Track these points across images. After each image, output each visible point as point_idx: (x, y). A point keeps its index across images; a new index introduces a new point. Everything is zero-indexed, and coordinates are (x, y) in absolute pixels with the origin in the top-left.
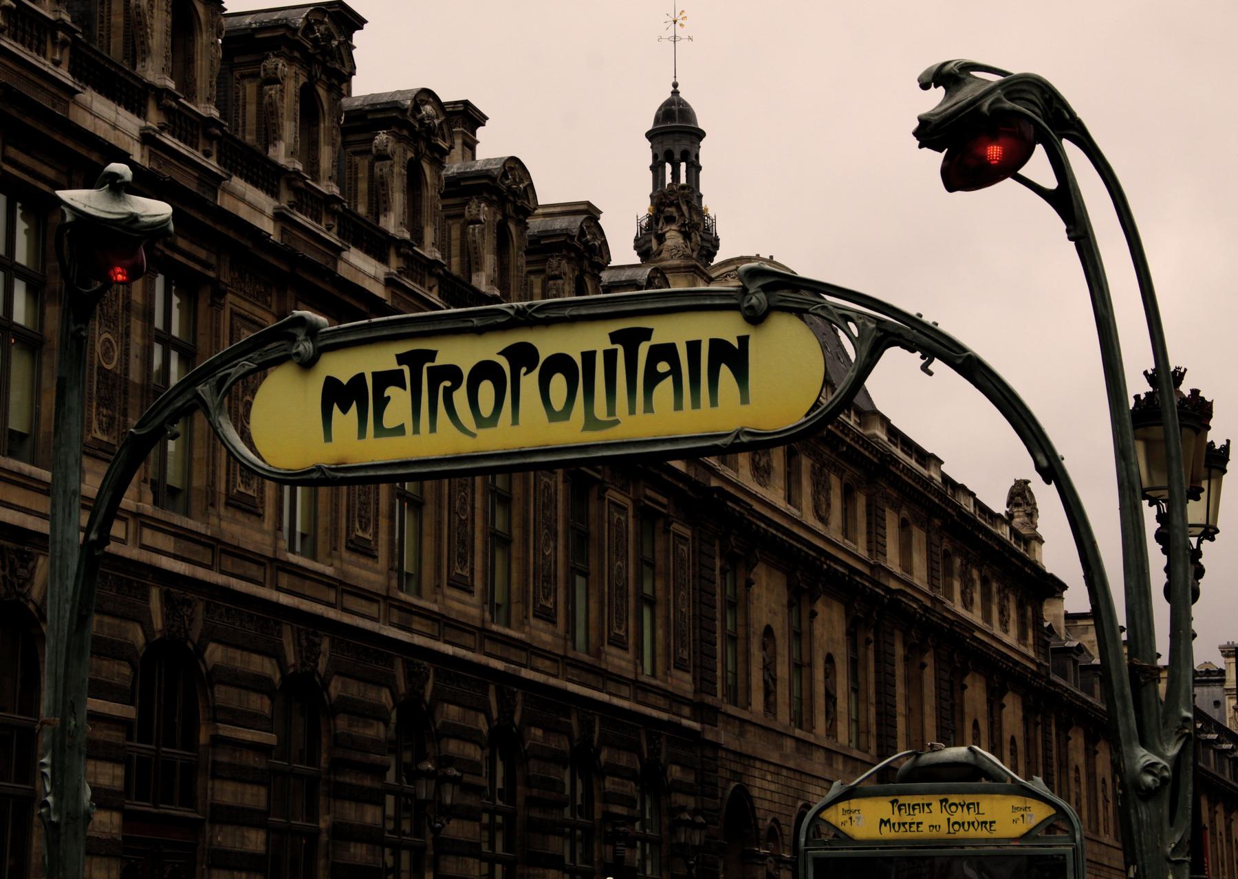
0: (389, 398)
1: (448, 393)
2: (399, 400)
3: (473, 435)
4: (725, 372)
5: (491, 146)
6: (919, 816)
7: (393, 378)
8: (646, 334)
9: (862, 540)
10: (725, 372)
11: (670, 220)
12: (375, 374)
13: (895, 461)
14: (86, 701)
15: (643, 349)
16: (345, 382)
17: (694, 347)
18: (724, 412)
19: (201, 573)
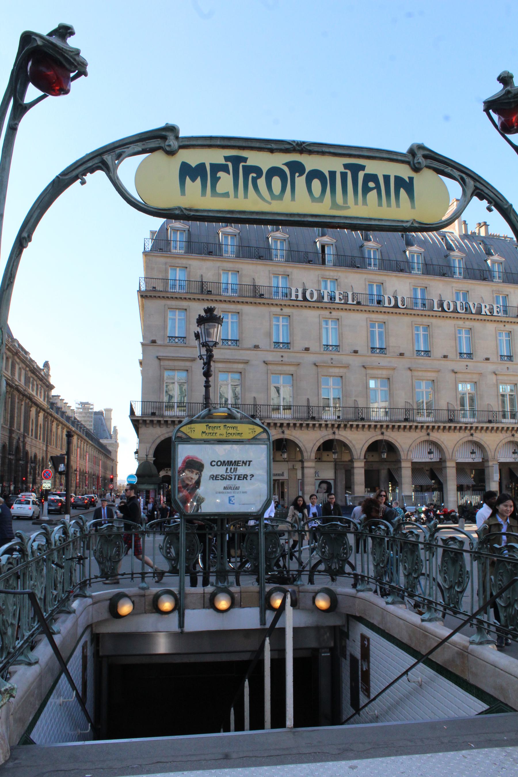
0: (220, 178)
1: (254, 180)
2: (225, 180)
3: (270, 203)
4: (402, 191)
6: (216, 431)
7: (224, 168)
8: (363, 168)
9: (10, 371)
10: (402, 191)
12: (212, 165)
13: (20, 352)
16: (193, 165)
17: (387, 178)
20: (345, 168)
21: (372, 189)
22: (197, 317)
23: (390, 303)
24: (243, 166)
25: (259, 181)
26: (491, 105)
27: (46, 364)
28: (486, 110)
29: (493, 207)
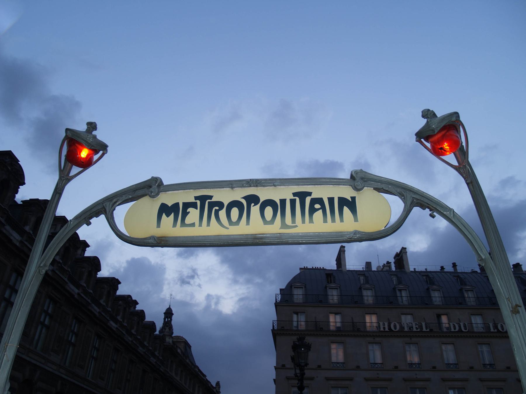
1: (217, 213)
2: (193, 214)
3: (228, 228)
4: (346, 209)
5: (138, 308)
8: (310, 194)
10: (346, 209)
11: (167, 326)
12: (184, 203)
15: (308, 200)
18: (347, 223)
19: (69, 379)
20: (294, 196)
21: (318, 209)
22: (292, 344)
23: (455, 329)
24: (209, 202)
25: (220, 212)
26: (421, 136)
27: (218, 384)
28: (419, 140)
29: (435, 214)
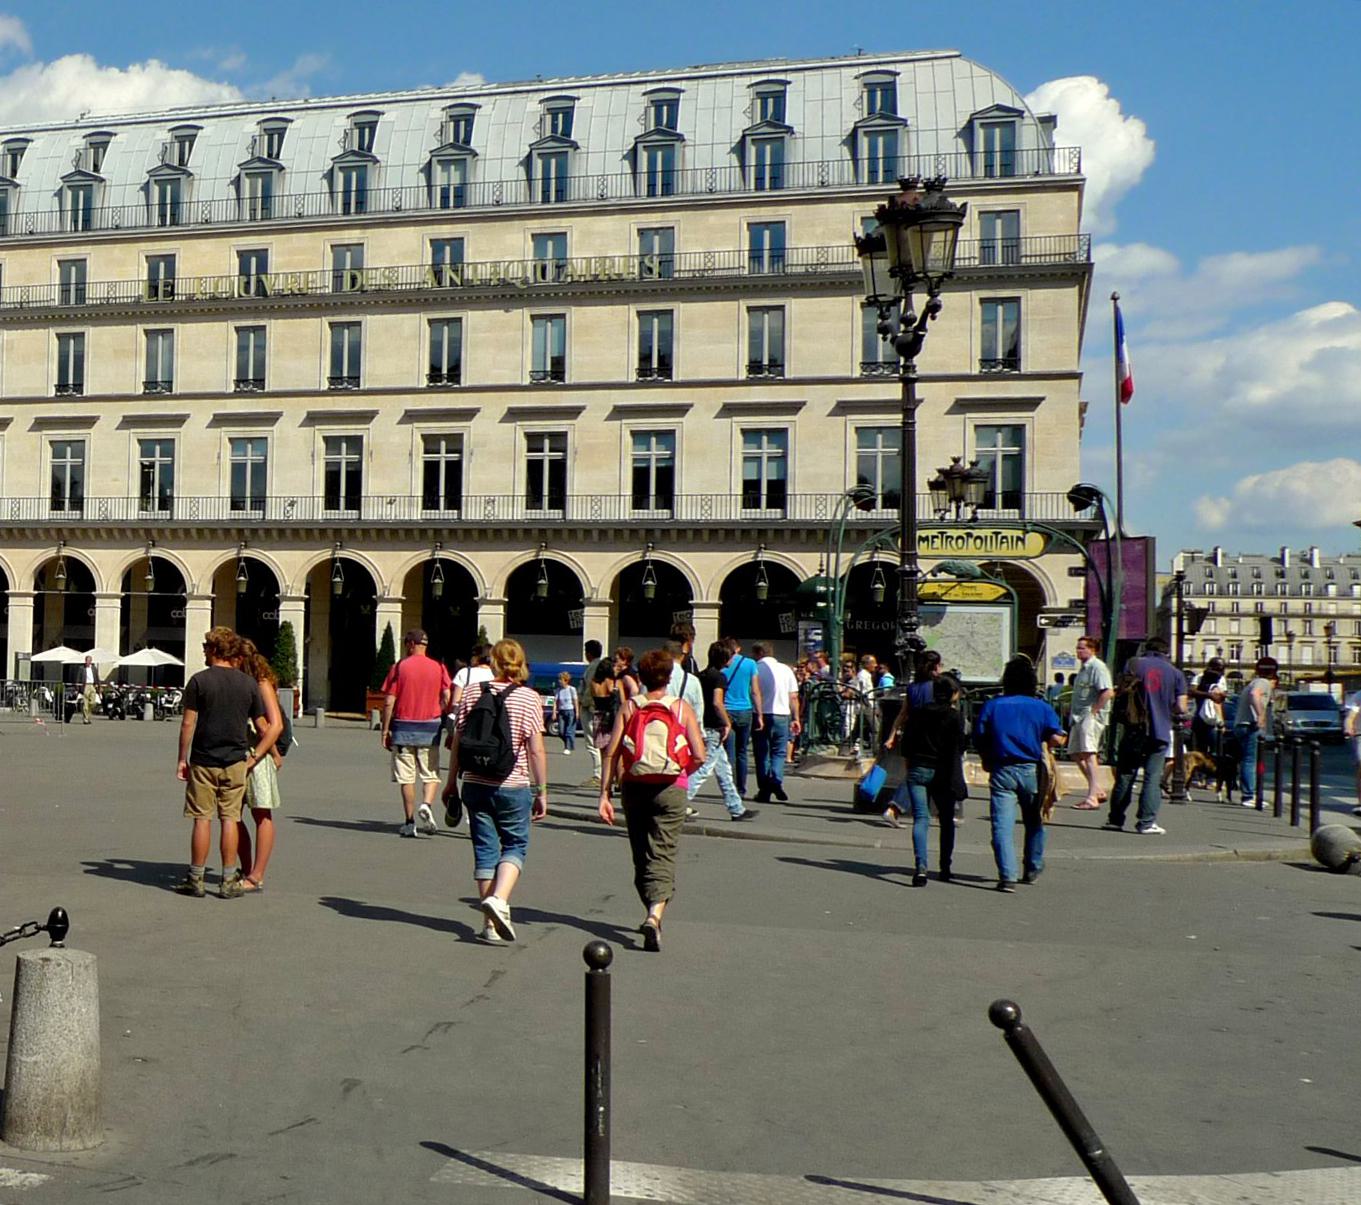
14: (723, 674)
15: (1000, 536)
